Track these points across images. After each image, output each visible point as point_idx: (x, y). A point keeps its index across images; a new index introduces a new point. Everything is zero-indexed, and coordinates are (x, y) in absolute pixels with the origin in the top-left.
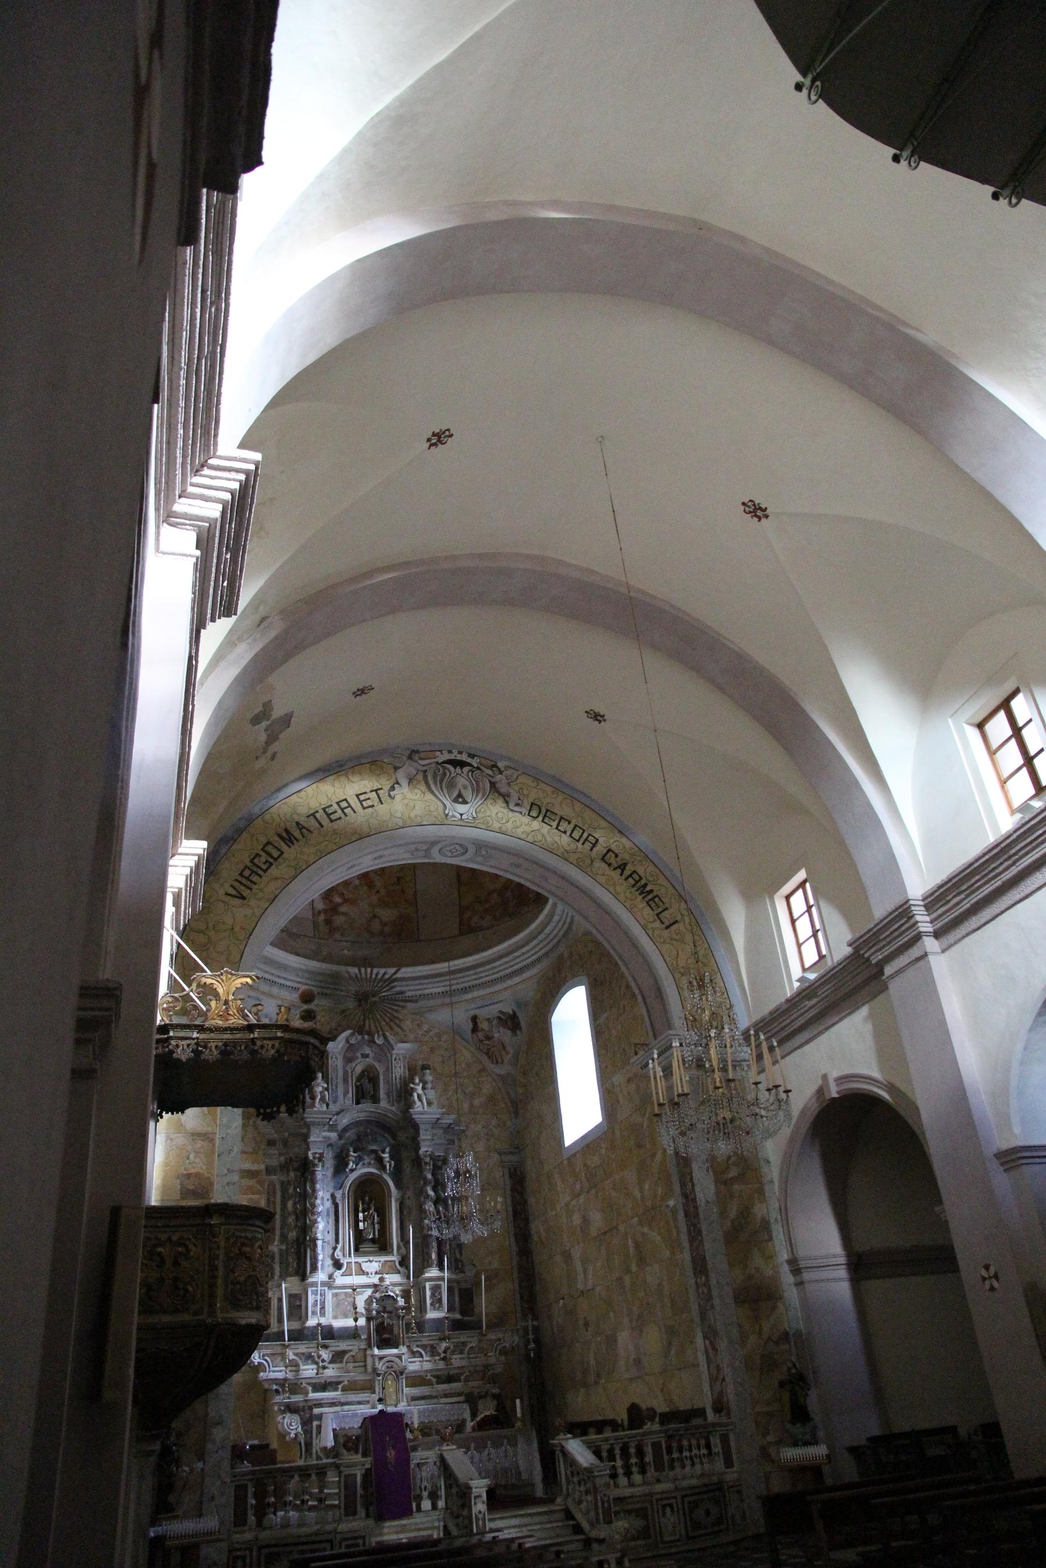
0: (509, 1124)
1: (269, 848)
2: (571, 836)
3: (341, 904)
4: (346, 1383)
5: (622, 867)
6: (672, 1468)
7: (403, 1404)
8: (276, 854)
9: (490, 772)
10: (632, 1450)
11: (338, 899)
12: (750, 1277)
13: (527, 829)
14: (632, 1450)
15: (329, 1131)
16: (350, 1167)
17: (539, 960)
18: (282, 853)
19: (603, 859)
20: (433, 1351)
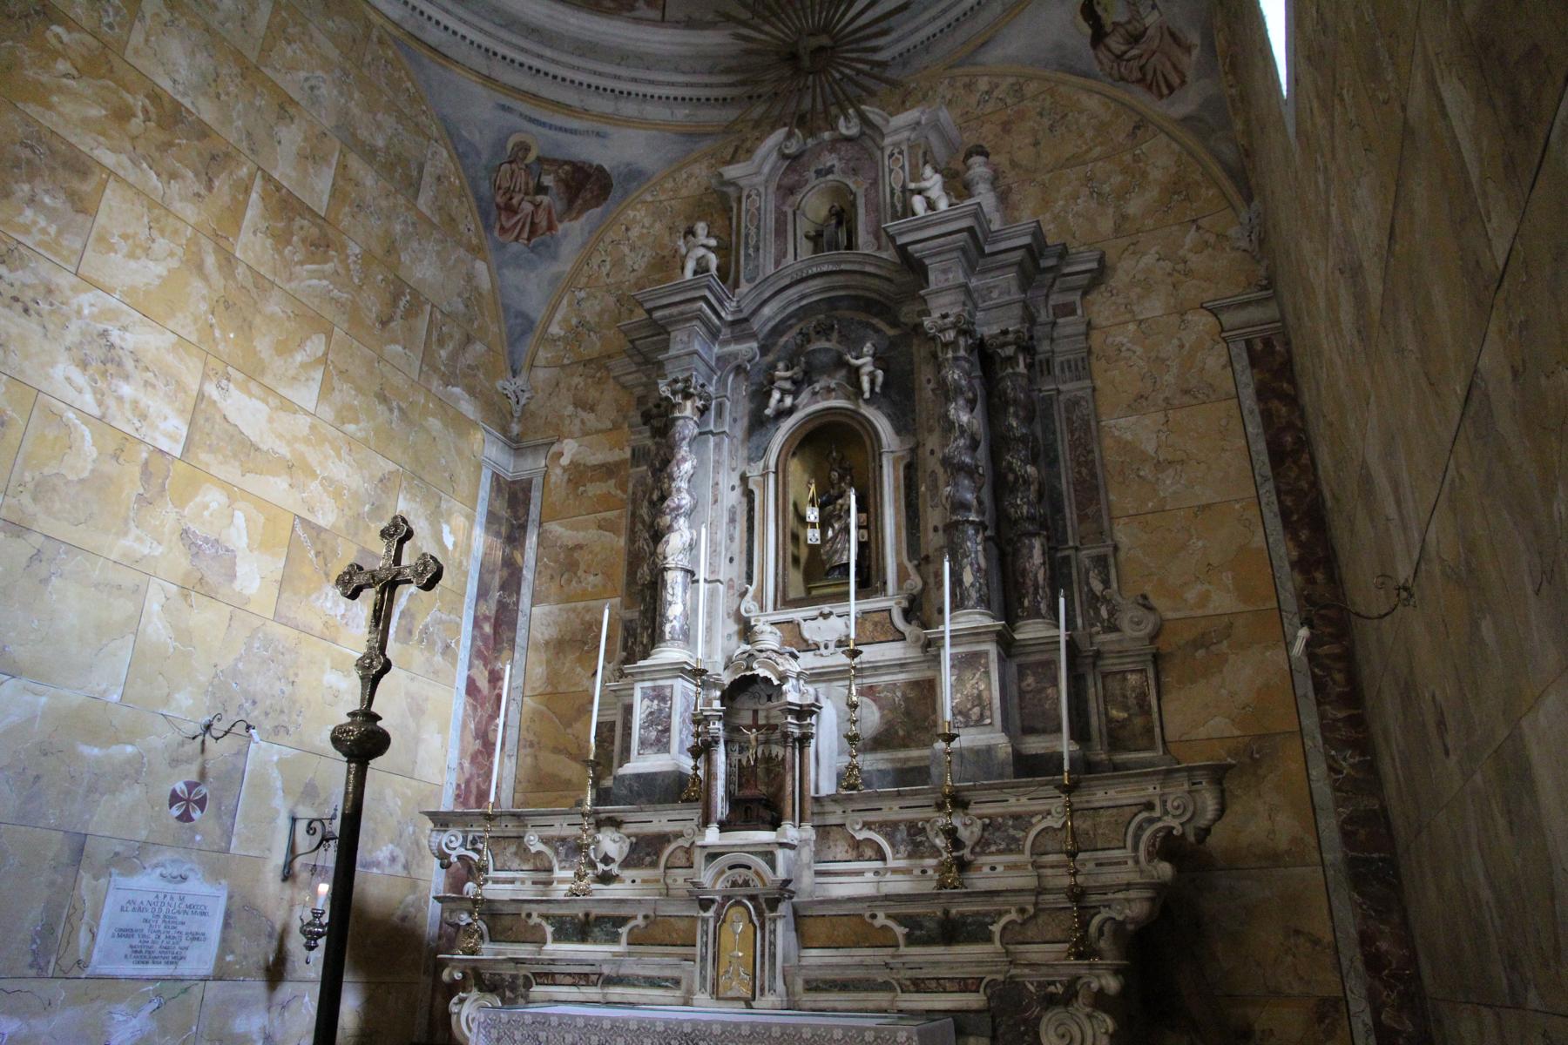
0: (1232, 232)
4: (640, 921)
7: (767, 1001)
15: (737, 339)
16: (773, 401)
20: (914, 839)
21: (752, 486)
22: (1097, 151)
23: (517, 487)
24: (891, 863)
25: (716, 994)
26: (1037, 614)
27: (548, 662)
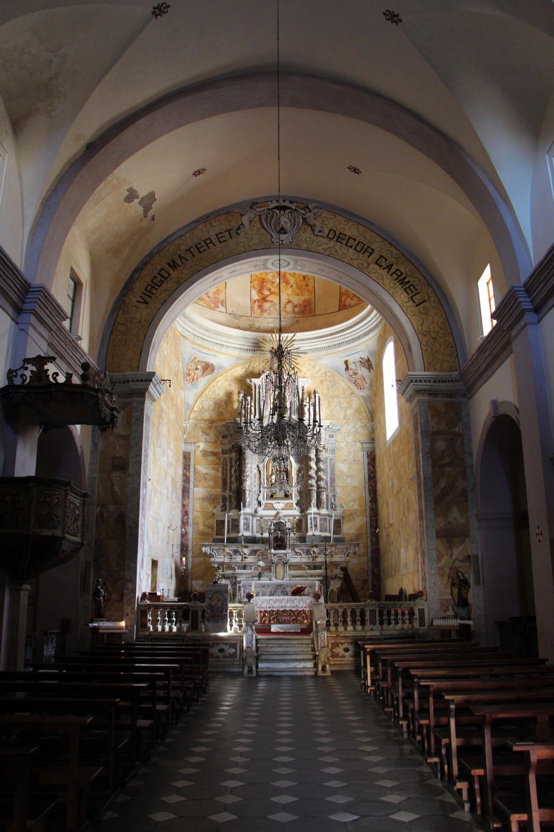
1: (163, 273)
2: (355, 249)
3: (269, 295)
5: (389, 267)
6: (381, 623)
7: (286, 579)
8: (166, 275)
9: (303, 212)
10: (358, 613)
11: (266, 293)
12: (450, 523)
13: (326, 247)
14: (358, 613)
17: (376, 326)
18: (170, 274)
19: (376, 263)
20: (308, 552)
21: (260, 469)
22: (342, 396)
23: (186, 454)
24: (303, 556)
25: (276, 578)
26: (323, 507)
27: (200, 503)
